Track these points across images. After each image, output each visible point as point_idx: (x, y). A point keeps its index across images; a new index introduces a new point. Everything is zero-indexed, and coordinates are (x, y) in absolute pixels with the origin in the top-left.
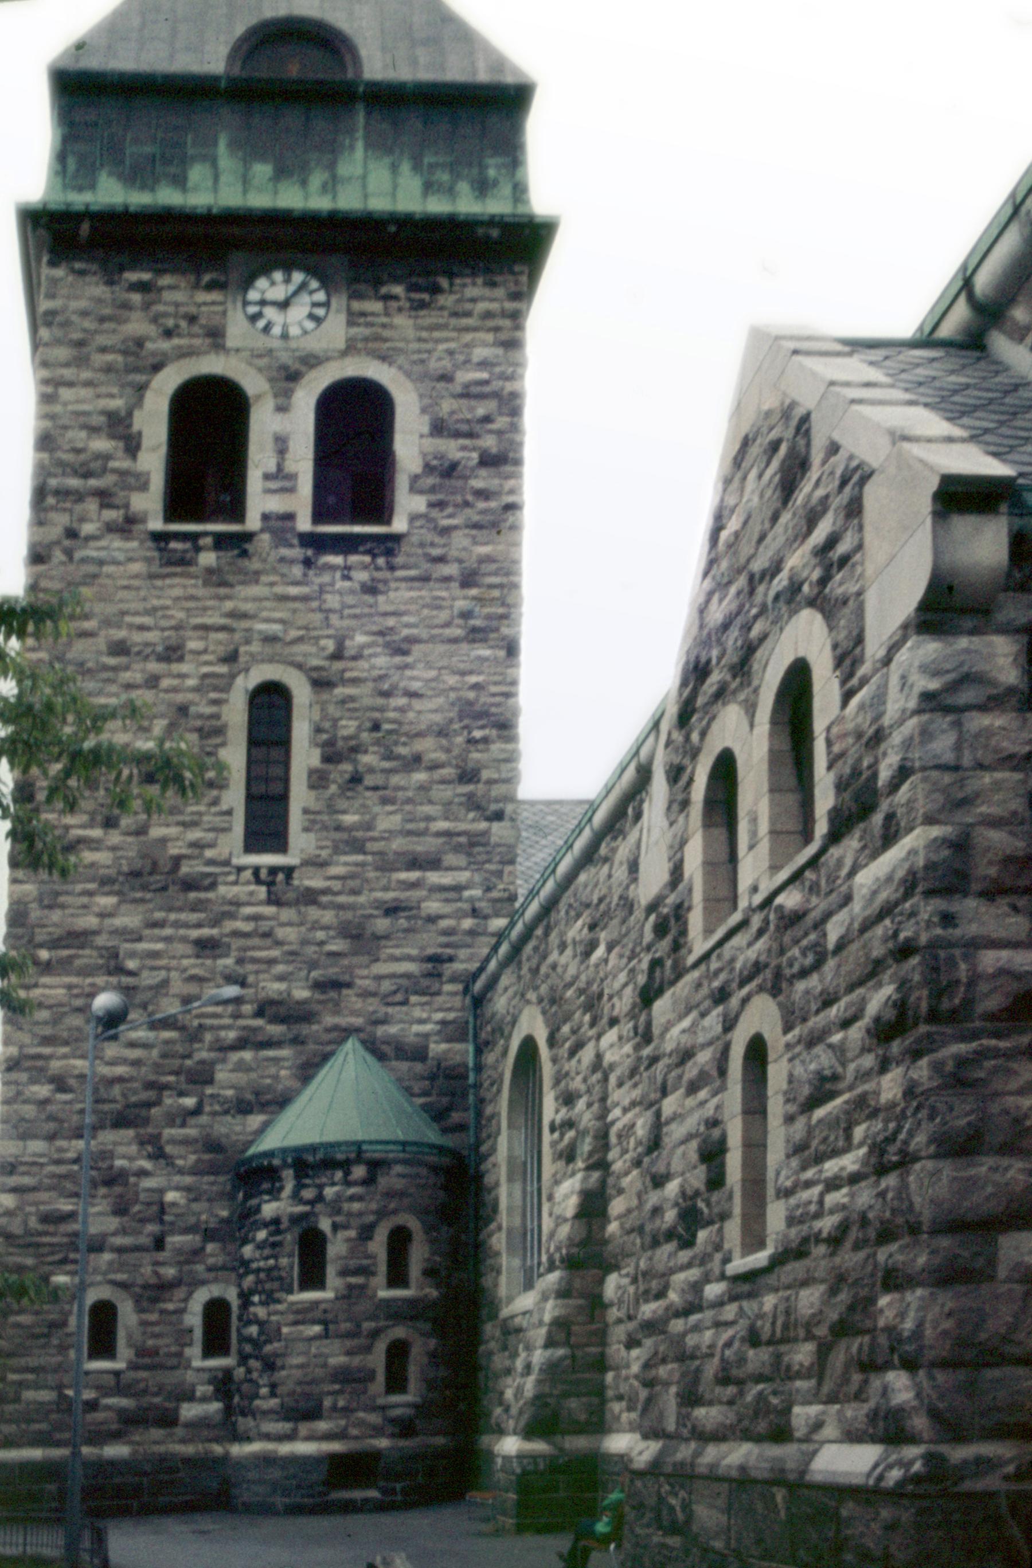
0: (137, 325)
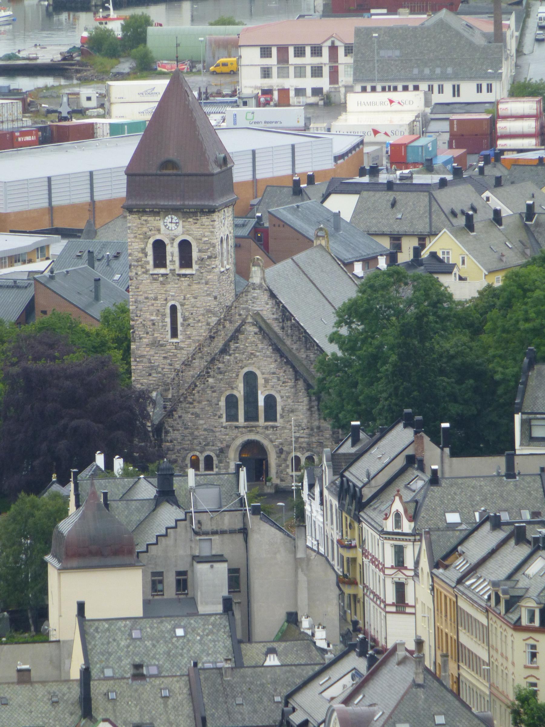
0: (145, 229)
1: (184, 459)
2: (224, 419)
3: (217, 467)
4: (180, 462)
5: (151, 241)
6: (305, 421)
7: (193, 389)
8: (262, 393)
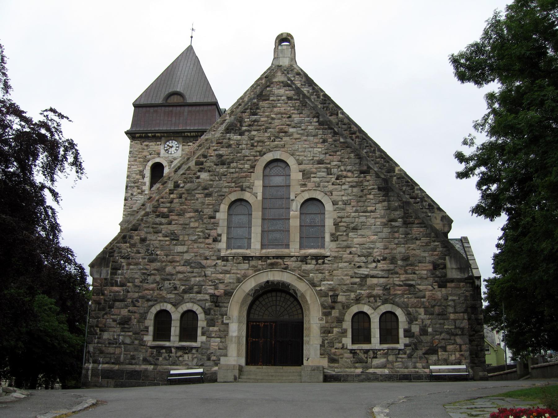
0: (146, 153)
1: (143, 317)
2: (222, 245)
3: (203, 334)
4: (134, 322)
5: (150, 164)
6: (380, 245)
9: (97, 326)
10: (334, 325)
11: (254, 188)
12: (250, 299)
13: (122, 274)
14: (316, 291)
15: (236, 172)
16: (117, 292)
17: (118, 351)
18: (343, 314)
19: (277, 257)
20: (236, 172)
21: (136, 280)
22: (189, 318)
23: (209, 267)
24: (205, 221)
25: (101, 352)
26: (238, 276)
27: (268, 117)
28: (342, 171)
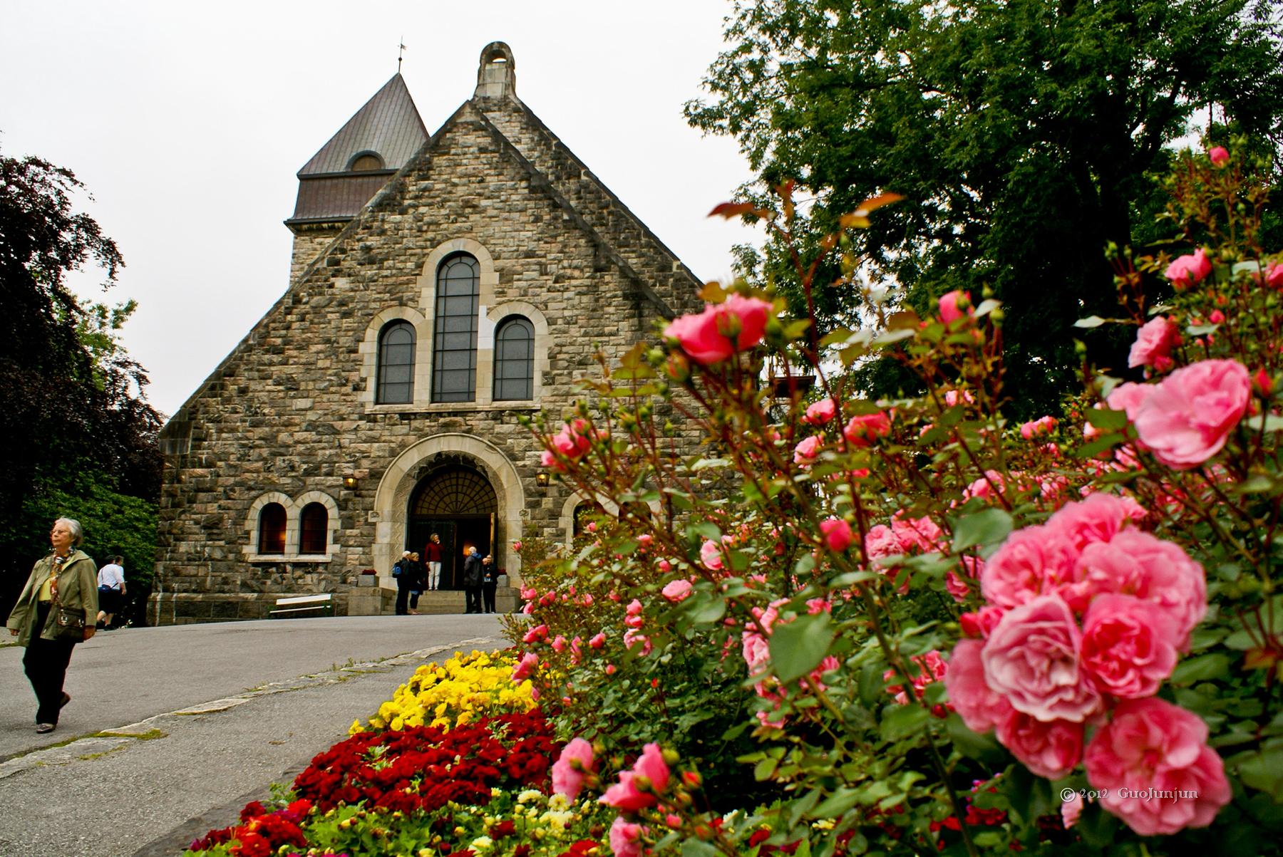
1: (242, 516)
2: (368, 395)
3: (336, 541)
4: (228, 524)
7: (289, 311)
8: (489, 311)
9: (170, 533)
10: (544, 522)
11: (420, 300)
12: (412, 484)
13: (209, 447)
14: (517, 467)
15: (393, 275)
16: (201, 476)
17: (202, 571)
18: (559, 505)
19: (455, 414)
20: (393, 275)
21: (232, 457)
22: (314, 515)
23: (345, 431)
24: (341, 357)
25: (177, 573)
26: (393, 445)
27: (445, 181)
28: (564, 268)
